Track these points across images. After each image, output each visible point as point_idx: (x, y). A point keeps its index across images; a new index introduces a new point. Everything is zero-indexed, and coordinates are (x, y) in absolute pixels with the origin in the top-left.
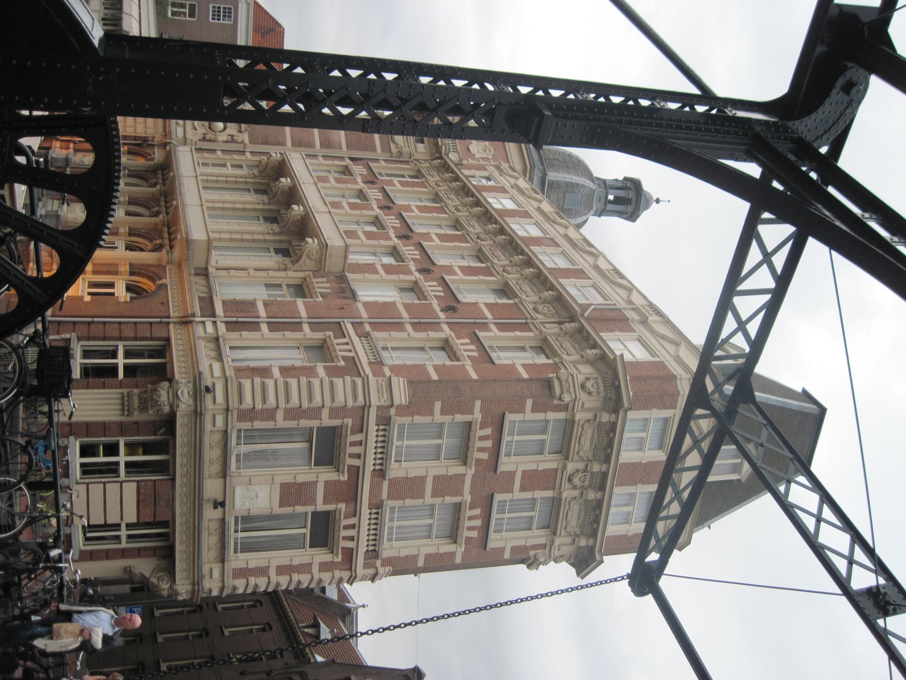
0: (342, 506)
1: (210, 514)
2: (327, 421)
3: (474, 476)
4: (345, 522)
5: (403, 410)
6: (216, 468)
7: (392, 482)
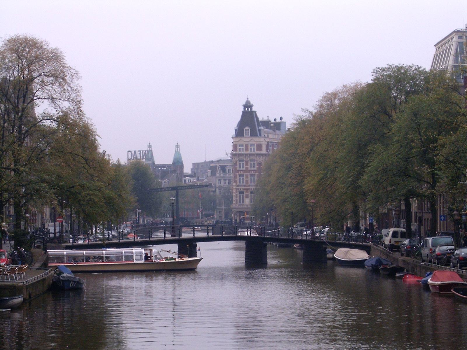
0: (249, 190)
1: (249, 206)
2: (238, 193)
3: (246, 173)
4: (251, 190)
5: (236, 184)
6: (244, 206)
7: (246, 184)
